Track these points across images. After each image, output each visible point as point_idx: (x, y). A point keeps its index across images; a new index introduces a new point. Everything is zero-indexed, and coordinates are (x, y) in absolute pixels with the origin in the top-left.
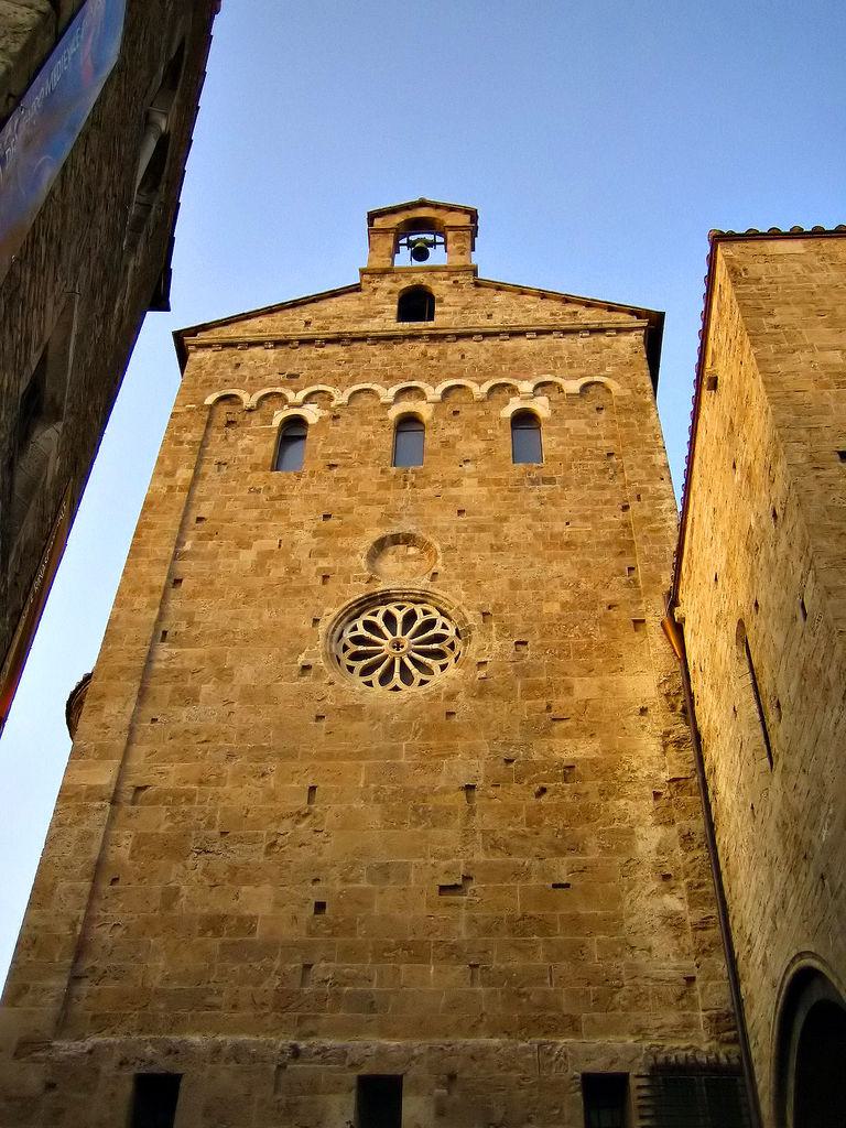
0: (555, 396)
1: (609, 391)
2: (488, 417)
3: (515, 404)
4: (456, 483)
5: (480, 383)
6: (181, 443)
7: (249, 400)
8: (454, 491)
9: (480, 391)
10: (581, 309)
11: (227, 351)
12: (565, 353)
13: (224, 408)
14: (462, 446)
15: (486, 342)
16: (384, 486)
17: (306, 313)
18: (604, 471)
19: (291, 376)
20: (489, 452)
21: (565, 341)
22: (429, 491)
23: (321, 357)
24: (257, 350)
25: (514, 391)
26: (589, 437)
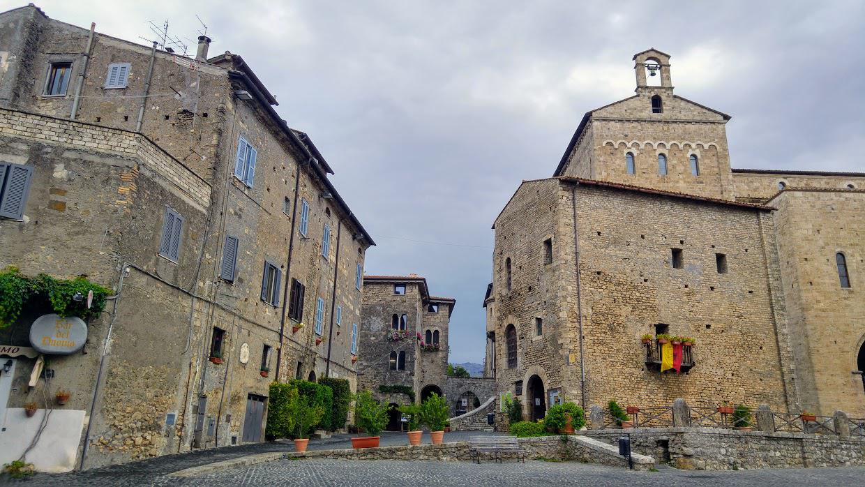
0: (702, 150)
1: (716, 148)
2: (683, 157)
3: (691, 152)
4: (678, 182)
5: (681, 143)
6: (600, 161)
8: (678, 185)
9: (681, 146)
10: (707, 111)
11: (604, 122)
12: (703, 132)
13: (608, 147)
15: (680, 125)
16: (659, 182)
19: (626, 136)
20: (685, 171)
21: (703, 126)
22: (671, 185)
24: (613, 122)
25: (690, 146)
26: (714, 167)
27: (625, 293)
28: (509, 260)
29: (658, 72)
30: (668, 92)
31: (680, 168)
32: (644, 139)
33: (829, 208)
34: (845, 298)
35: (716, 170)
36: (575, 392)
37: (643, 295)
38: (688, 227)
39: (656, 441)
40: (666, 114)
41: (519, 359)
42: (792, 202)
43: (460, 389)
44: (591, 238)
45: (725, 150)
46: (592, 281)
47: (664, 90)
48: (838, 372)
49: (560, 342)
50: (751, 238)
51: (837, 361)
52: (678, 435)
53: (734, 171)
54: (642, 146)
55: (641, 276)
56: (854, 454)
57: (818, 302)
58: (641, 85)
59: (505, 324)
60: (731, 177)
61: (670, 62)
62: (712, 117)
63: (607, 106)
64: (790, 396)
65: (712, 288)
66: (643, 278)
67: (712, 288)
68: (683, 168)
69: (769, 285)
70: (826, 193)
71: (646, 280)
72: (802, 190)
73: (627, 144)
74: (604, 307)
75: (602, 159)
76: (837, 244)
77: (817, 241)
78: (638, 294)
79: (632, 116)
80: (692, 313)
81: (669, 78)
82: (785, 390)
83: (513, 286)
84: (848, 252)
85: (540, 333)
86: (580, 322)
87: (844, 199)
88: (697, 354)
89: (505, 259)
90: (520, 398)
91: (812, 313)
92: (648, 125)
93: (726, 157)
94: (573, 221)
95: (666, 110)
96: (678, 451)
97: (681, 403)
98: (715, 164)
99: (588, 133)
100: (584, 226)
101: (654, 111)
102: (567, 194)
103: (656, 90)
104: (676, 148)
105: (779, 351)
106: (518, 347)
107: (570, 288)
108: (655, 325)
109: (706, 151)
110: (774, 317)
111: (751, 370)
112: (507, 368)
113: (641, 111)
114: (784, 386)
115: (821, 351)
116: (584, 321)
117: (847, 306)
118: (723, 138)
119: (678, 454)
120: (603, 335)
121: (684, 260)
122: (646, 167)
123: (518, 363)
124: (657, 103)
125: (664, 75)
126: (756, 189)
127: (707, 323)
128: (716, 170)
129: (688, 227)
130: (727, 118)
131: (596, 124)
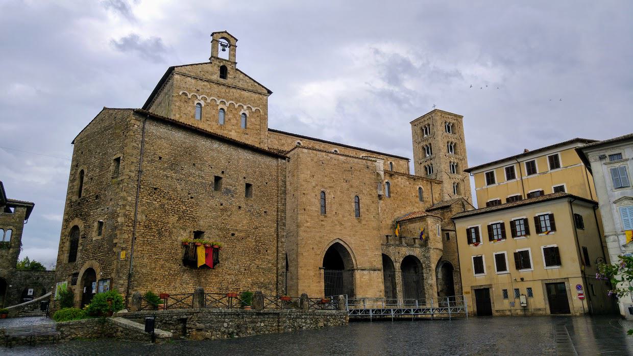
0: (250, 111)
2: (237, 114)
3: (242, 111)
4: (231, 131)
5: (236, 104)
7: (189, 96)
8: (230, 133)
9: (236, 106)
10: (257, 85)
11: (183, 77)
13: (184, 96)
14: (232, 121)
16: (217, 128)
17: (200, 68)
18: (257, 134)
20: (237, 124)
21: (253, 95)
23: (204, 85)
25: (243, 107)
27: (174, 206)
28: (82, 172)
29: (227, 49)
30: (233, 66)
31: (234, 121)
32: (211, 95)
33: (321, 163)
34: (322, 221)
35: (258, 127)
36: (122, 282)
37: (188, 209)
38: (229, 162)
39: (178, 320)
40: (229, 81)
41: (79, 254)
42: (301, 155)
43: (28, 281)
44: (152, 161)
45: (266, 114)
46: (149, 195)
47: (230, 63)
48: (311, 268)
49: (115, 242)
50: (271, 175)
51: (312, 261)
52: (195, 314)
53: (269, 130)
54: (209, 101)
55: (189, 194)
56: (308, 321)
57: (307, 222)
58: (215, 55)
59: (71, 225)
60: (267, 133)
61: (237, 44)
62: (260, 89)
63: (187, 65)
64: (280, 284)
65: (240, 207)
66: (189, 196)
67: (240, 207)
68: (236, 122)
69: (278, 208)
70: (320, 153)
71: (192, 198)
72: (307, 148)
73: (198, 96)
74: (156, 215)
75: (177, 104)
76: (322, 186)
77: (311, 182)
78: (184, 208)
79: (204, 77)
80: (223, 224)
81: (235, 56)
82: (277, 280)
83: (83, 194)
84: (327, 191)
85: (100, 234)
86: (134, 227)
87: (329, 158)
88: (223, 255)
89: (79, 171)
90: (74, 287)
91: (302, 229)
92: (215, 86)
93: (266, 119)
94: (140, 146)
95: (230, 78)
96: (193, 326)
97: (200, 290)
98: (258, 123)
99: (169, 83)
100: (149, 151)
101: (221, 77)
102: (138, 123)
103: (224, 62)
104: (233, 107)
105: (278, 253)
106: (79, 245)
107: (129, 199)
108: (194, 232)
109: (253, 112)
110: (277, 230)
111: (258, 266)
112: (67, 262)
113: (212, 74)
114: (277, 277)
115: (304, 254)
116: (138, 226)
117: (322, 225)
118: (265, 106)
119: (192, 328)
120: (152, 237)
121: (223, 186)
122: (209, 116)
123: (77, 258)
124: (224, 72)
125: (232, 52)
126: (283, 145)
127: (233, 232)
128: (258, 127)
129: (229, 162)
130: (270, 92)
131: (176, 77)
